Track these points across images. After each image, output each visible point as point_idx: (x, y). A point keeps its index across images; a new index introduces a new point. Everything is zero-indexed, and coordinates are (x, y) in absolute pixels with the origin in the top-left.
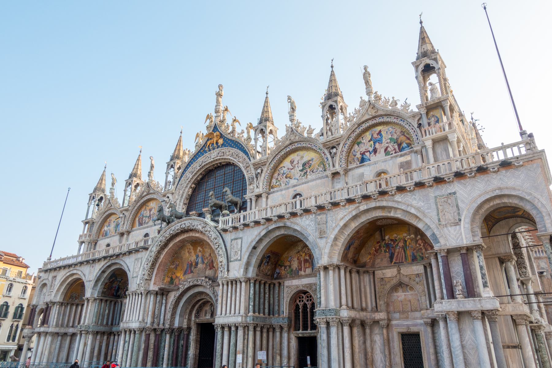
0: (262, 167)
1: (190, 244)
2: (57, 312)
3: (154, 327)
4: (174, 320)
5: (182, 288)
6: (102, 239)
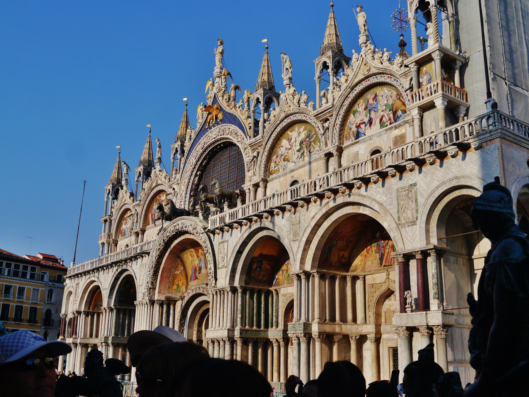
6: (121, 239)
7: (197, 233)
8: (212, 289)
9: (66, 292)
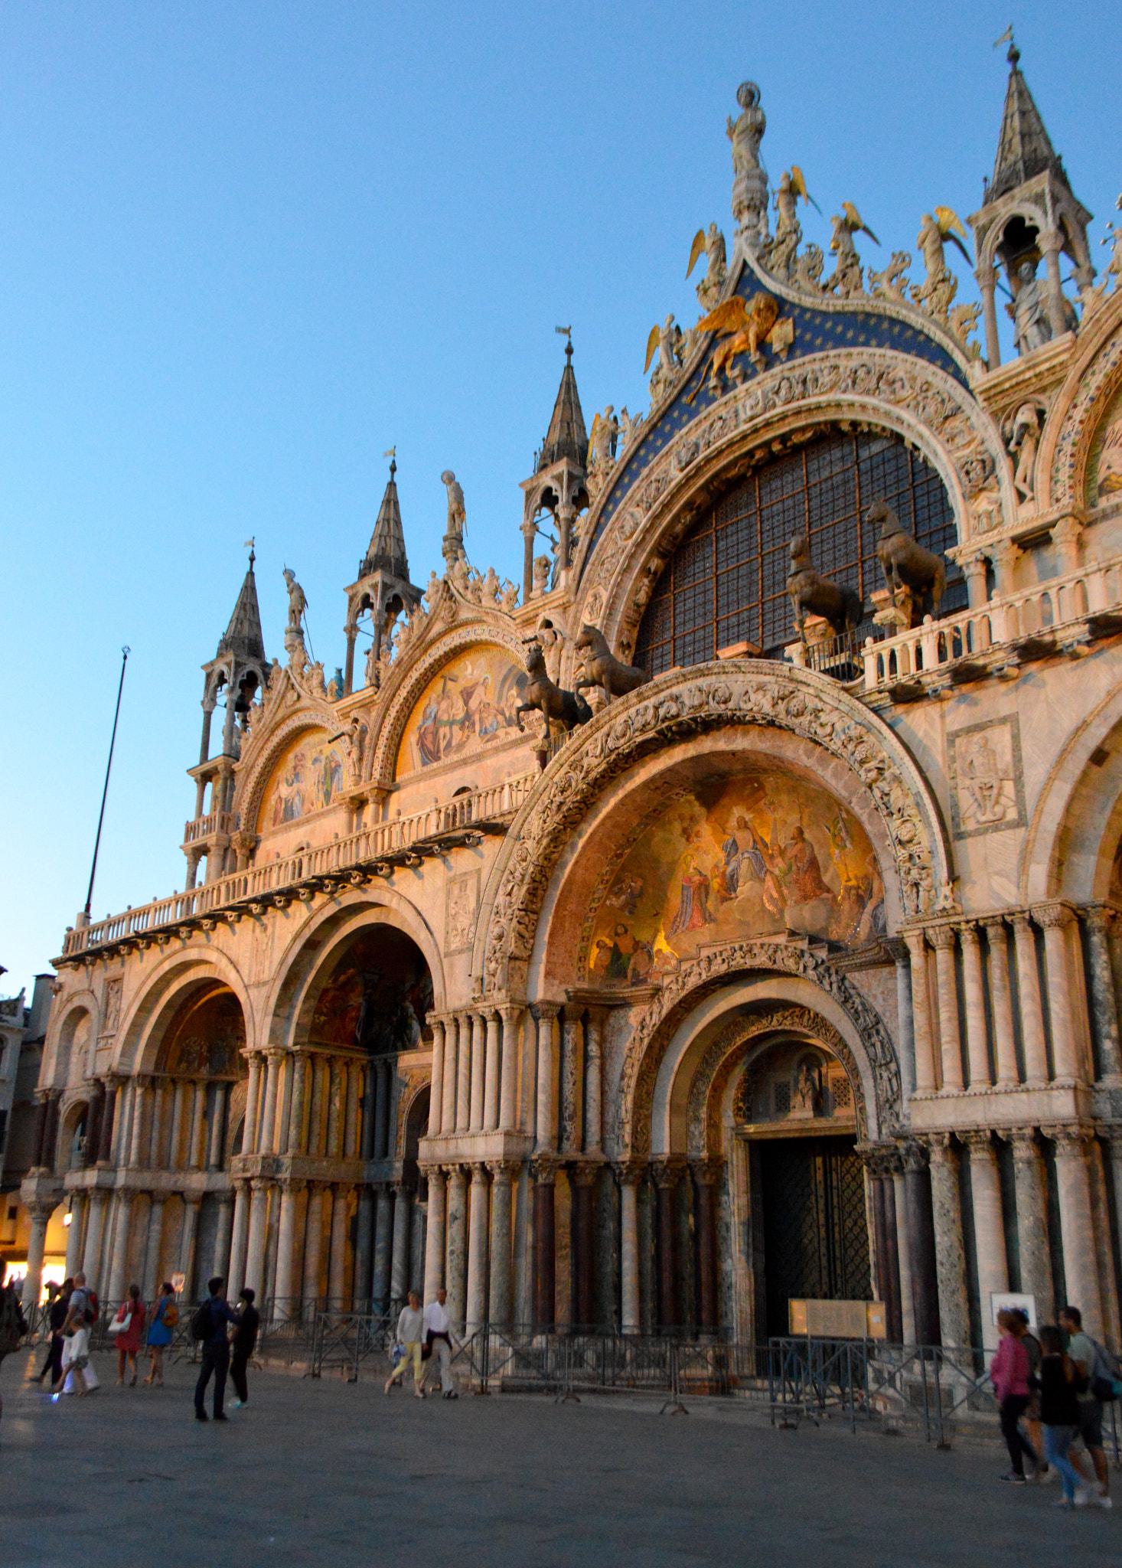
0: (1042, 398)
1: (692, 798)
2: (137, 1114)
3: (563, 1158)
4: (645, 1125)
5: (674, 987)
6: (274, 833)
7: (799, 714)
8: (927, 924)
9: (60, 1012)
